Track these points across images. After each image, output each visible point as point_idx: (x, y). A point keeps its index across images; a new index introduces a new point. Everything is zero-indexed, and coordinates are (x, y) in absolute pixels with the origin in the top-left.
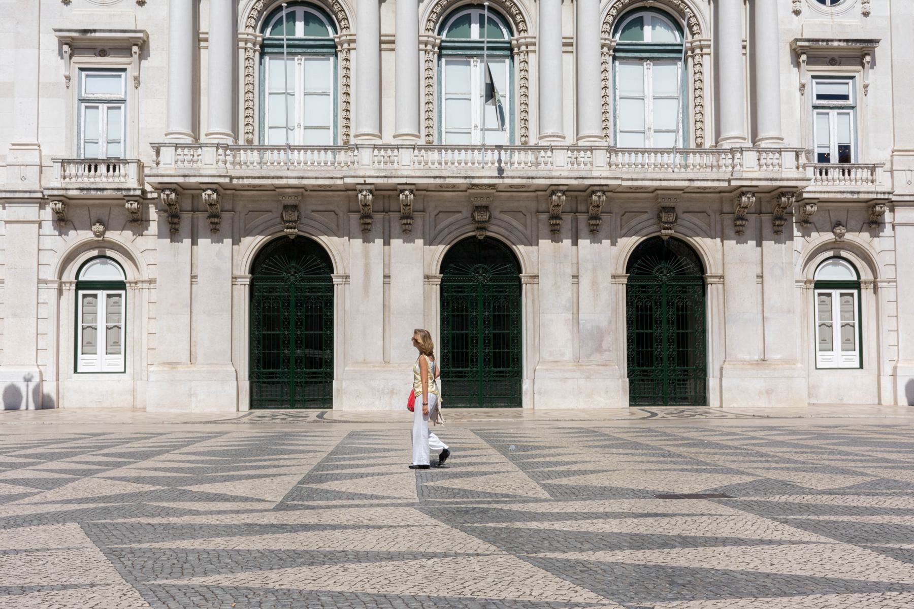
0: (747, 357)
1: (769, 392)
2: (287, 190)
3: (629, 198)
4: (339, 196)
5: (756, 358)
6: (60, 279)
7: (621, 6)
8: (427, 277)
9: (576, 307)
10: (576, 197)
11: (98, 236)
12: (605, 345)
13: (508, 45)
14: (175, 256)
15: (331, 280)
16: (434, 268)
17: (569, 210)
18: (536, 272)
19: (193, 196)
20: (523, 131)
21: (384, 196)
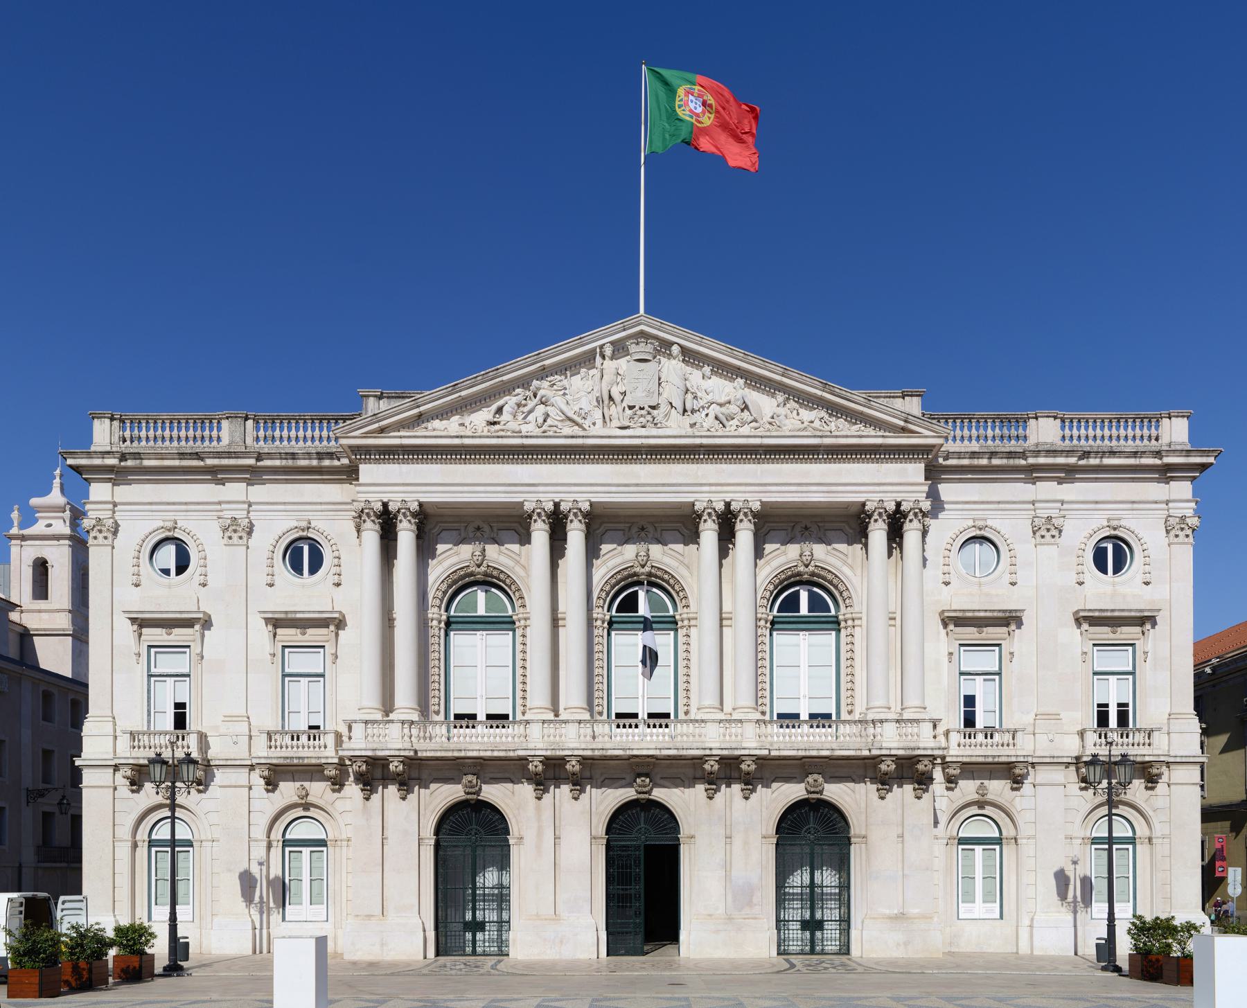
0: (887, 912)
1: (906, 944)
2: (467, 761)
3: (780, 765)
4: (515, 764)
5: (896, 912)
6: (269, 837)
7: (777, 581)
8: (593, 838)
9: (727, 866)
10: (730, 764)
11: (302, 799)
12: (755, 900)
13: (673, 619)
14: (367, 820)
15: (507, 840)
16: (600, 830)
17: (723, 776)
18: (692, 833)
19: (383, 765)
20: (685, 700)
21: (555, 765)
